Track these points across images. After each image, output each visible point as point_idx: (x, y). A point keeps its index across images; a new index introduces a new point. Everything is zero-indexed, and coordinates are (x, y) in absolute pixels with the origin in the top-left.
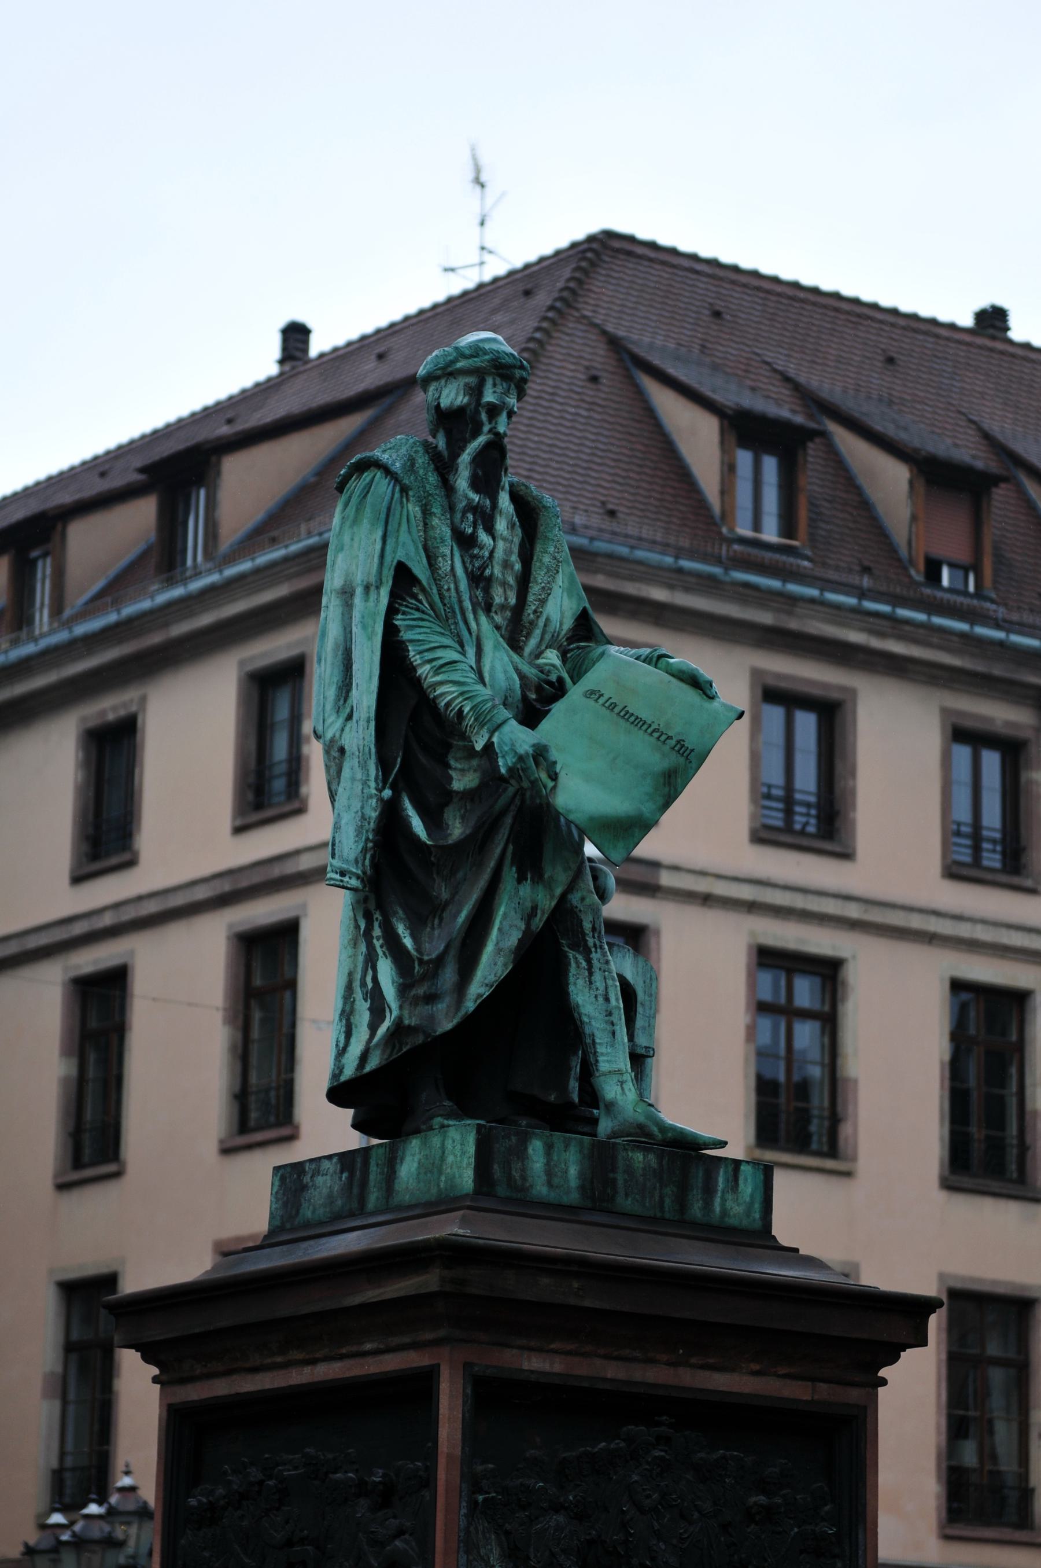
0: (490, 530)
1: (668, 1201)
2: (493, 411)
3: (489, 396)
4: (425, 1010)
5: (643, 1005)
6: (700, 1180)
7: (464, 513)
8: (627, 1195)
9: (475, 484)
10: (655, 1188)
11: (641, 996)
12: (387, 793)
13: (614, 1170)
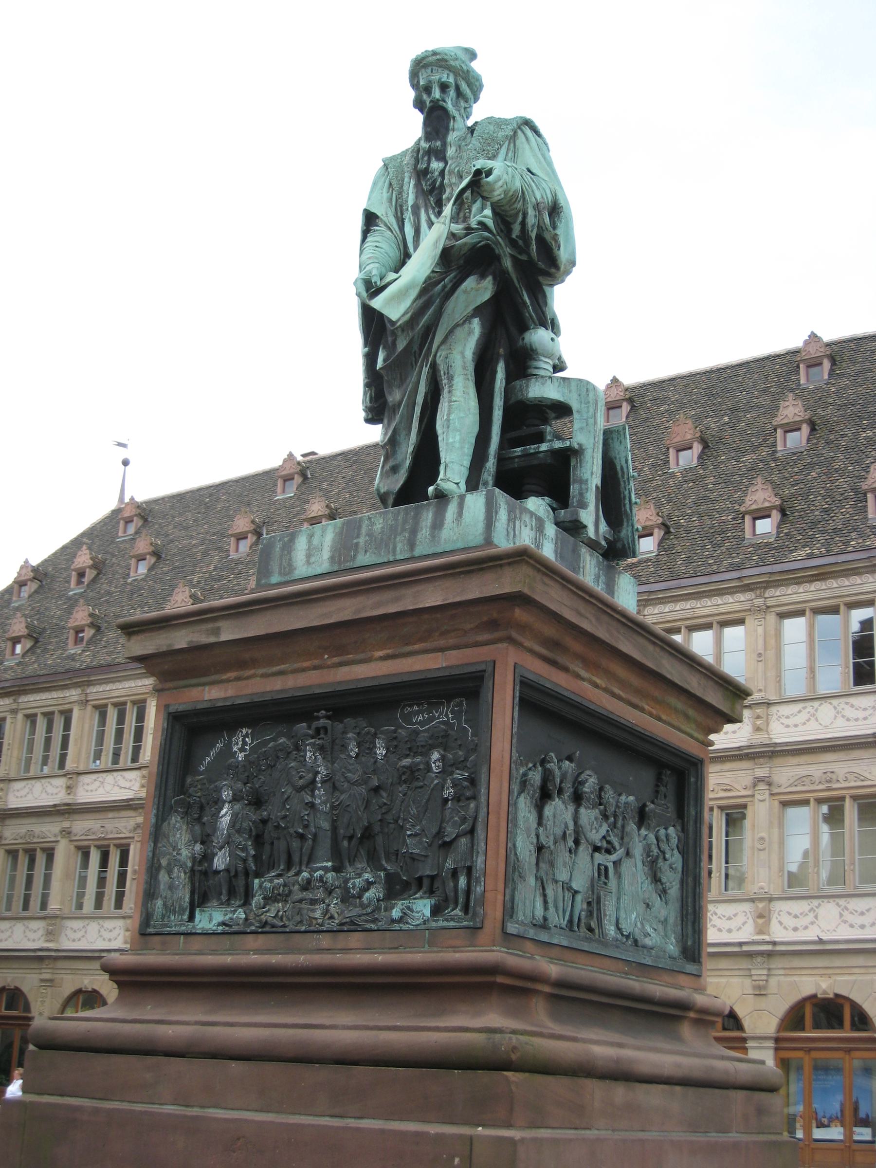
1: (399, 546)
5: (578, 412)
6: (430, 521)
7: (423, 157)
8: (366, 551)
10: (390, 539)
11: (575, 406)
12: (367, 349)
13: (358, 536)
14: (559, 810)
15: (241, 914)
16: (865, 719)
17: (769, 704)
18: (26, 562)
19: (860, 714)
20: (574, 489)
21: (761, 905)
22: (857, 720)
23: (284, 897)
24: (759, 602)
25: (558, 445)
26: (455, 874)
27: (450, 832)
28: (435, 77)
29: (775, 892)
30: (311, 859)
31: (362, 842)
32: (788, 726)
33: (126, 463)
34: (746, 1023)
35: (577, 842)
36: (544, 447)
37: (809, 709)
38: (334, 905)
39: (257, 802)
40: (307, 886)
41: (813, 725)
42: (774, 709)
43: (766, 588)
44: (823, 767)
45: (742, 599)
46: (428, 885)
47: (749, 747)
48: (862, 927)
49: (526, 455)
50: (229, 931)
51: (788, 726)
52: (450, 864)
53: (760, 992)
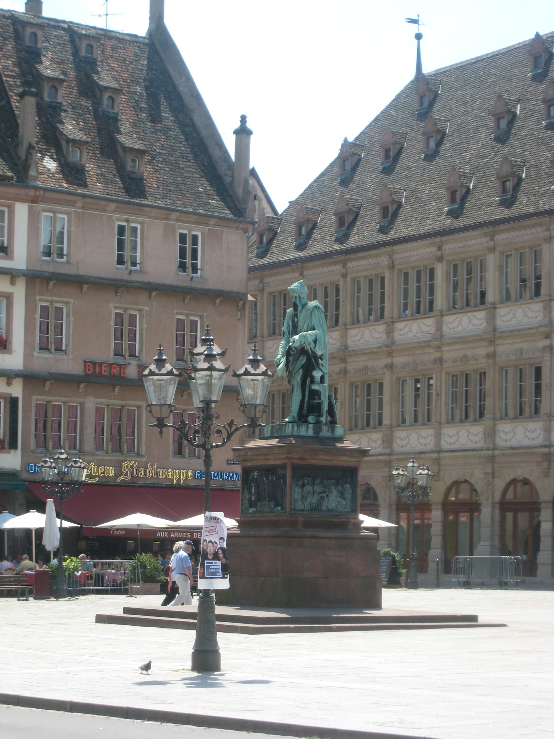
14: (308, 488)
18: (346, 140)
33: (419, 37)
35: (314, 493)
36: (315, 401)
50: (254, 513)
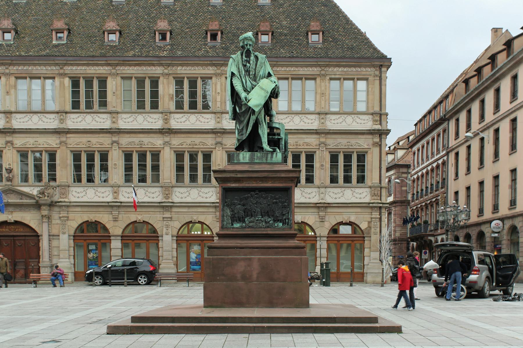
0: (249, 63)
2: (247, 45)
3: (245, 43)
4: (241, 136)
9: (246, 57)
15: (244, 225)
16: (155, 122)
17: (118, 113)
19: (154, 121)
20: (281, 146)
21: (115, 189)
22: (152, 123)
23: (253, 222)
24: (114, 71)
25: (279, 137)
26: (285, 219)
27: (284, 213)
28: (249, 43)
29: (121, 184)
30: (257, 215)
31: (267, 214)
32: (125, 122)
34: (110, 231)
36: (276, 137)
37: (134, 116)
38: (264, 223)
39: (244, 205)
40: (257, 220)
41: (135, 123)
42: (120, 115)
43: (116, 66)
44: (139, 139)
45: (107, 69)
46: (281, 221)
47: (110, 129)
48: (153, 198)
49: (272, 138)
50: (242, 227)
51: (125, 122)
52: (284, 218)
53: (115, 220)
